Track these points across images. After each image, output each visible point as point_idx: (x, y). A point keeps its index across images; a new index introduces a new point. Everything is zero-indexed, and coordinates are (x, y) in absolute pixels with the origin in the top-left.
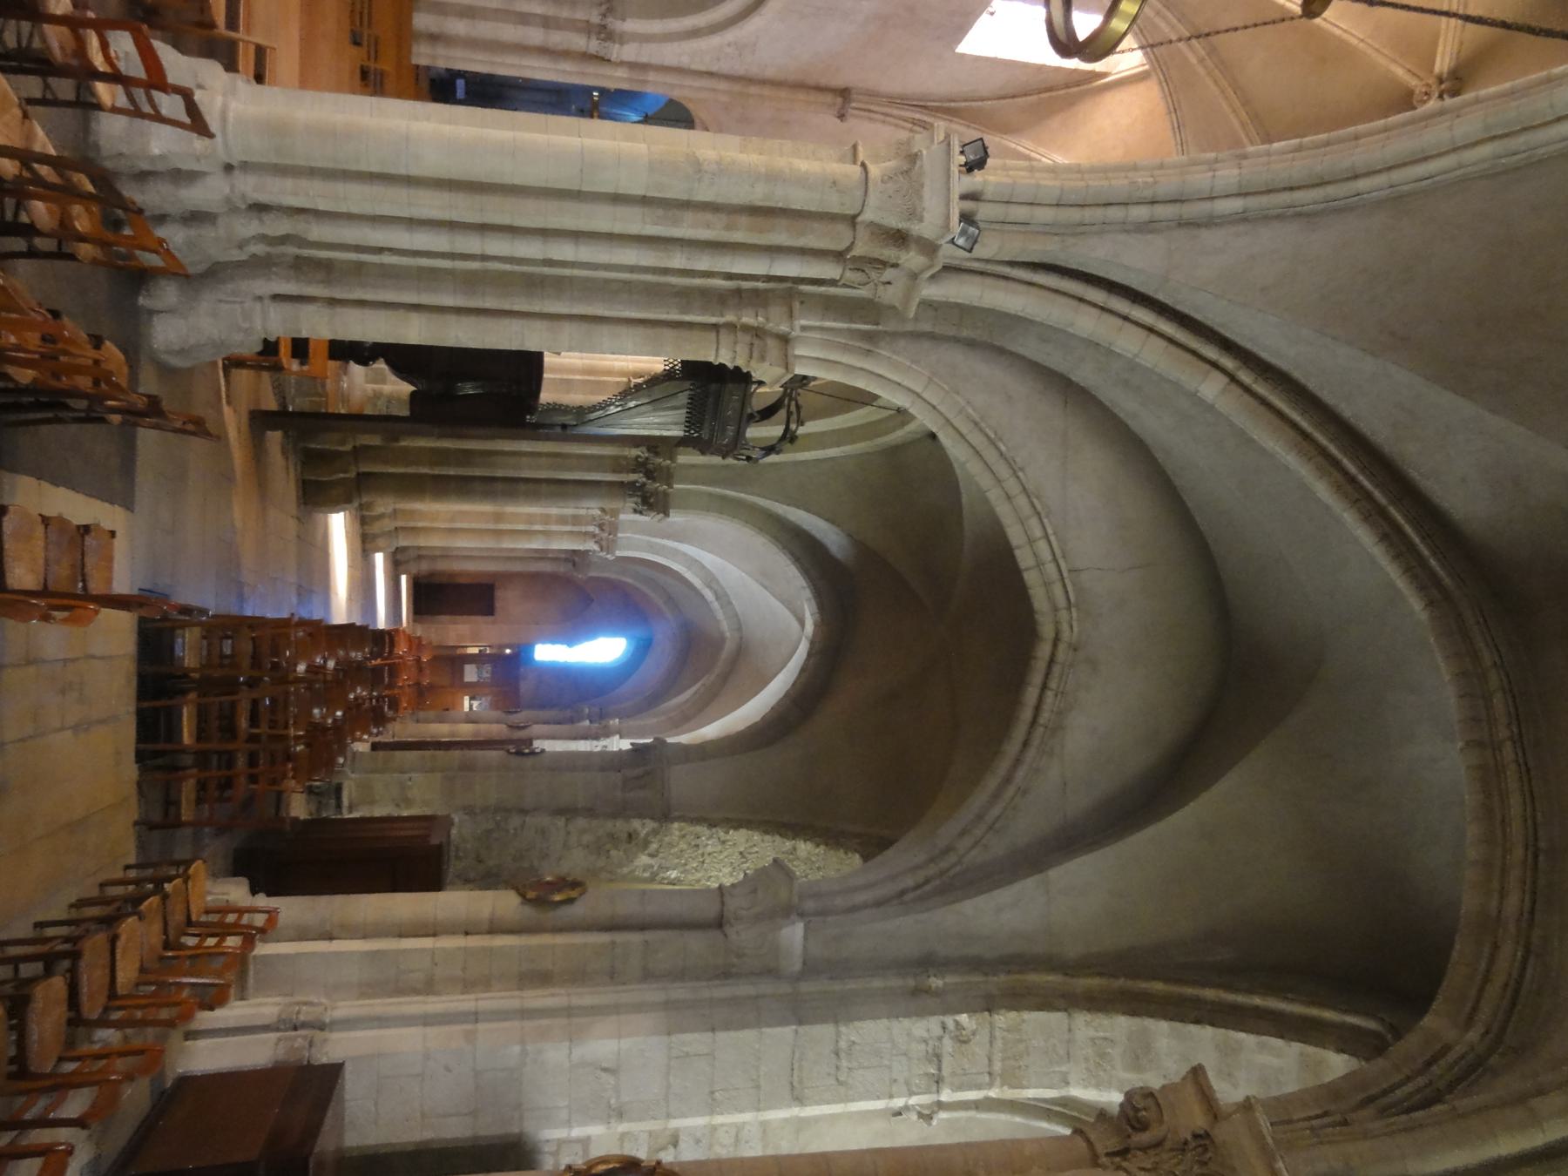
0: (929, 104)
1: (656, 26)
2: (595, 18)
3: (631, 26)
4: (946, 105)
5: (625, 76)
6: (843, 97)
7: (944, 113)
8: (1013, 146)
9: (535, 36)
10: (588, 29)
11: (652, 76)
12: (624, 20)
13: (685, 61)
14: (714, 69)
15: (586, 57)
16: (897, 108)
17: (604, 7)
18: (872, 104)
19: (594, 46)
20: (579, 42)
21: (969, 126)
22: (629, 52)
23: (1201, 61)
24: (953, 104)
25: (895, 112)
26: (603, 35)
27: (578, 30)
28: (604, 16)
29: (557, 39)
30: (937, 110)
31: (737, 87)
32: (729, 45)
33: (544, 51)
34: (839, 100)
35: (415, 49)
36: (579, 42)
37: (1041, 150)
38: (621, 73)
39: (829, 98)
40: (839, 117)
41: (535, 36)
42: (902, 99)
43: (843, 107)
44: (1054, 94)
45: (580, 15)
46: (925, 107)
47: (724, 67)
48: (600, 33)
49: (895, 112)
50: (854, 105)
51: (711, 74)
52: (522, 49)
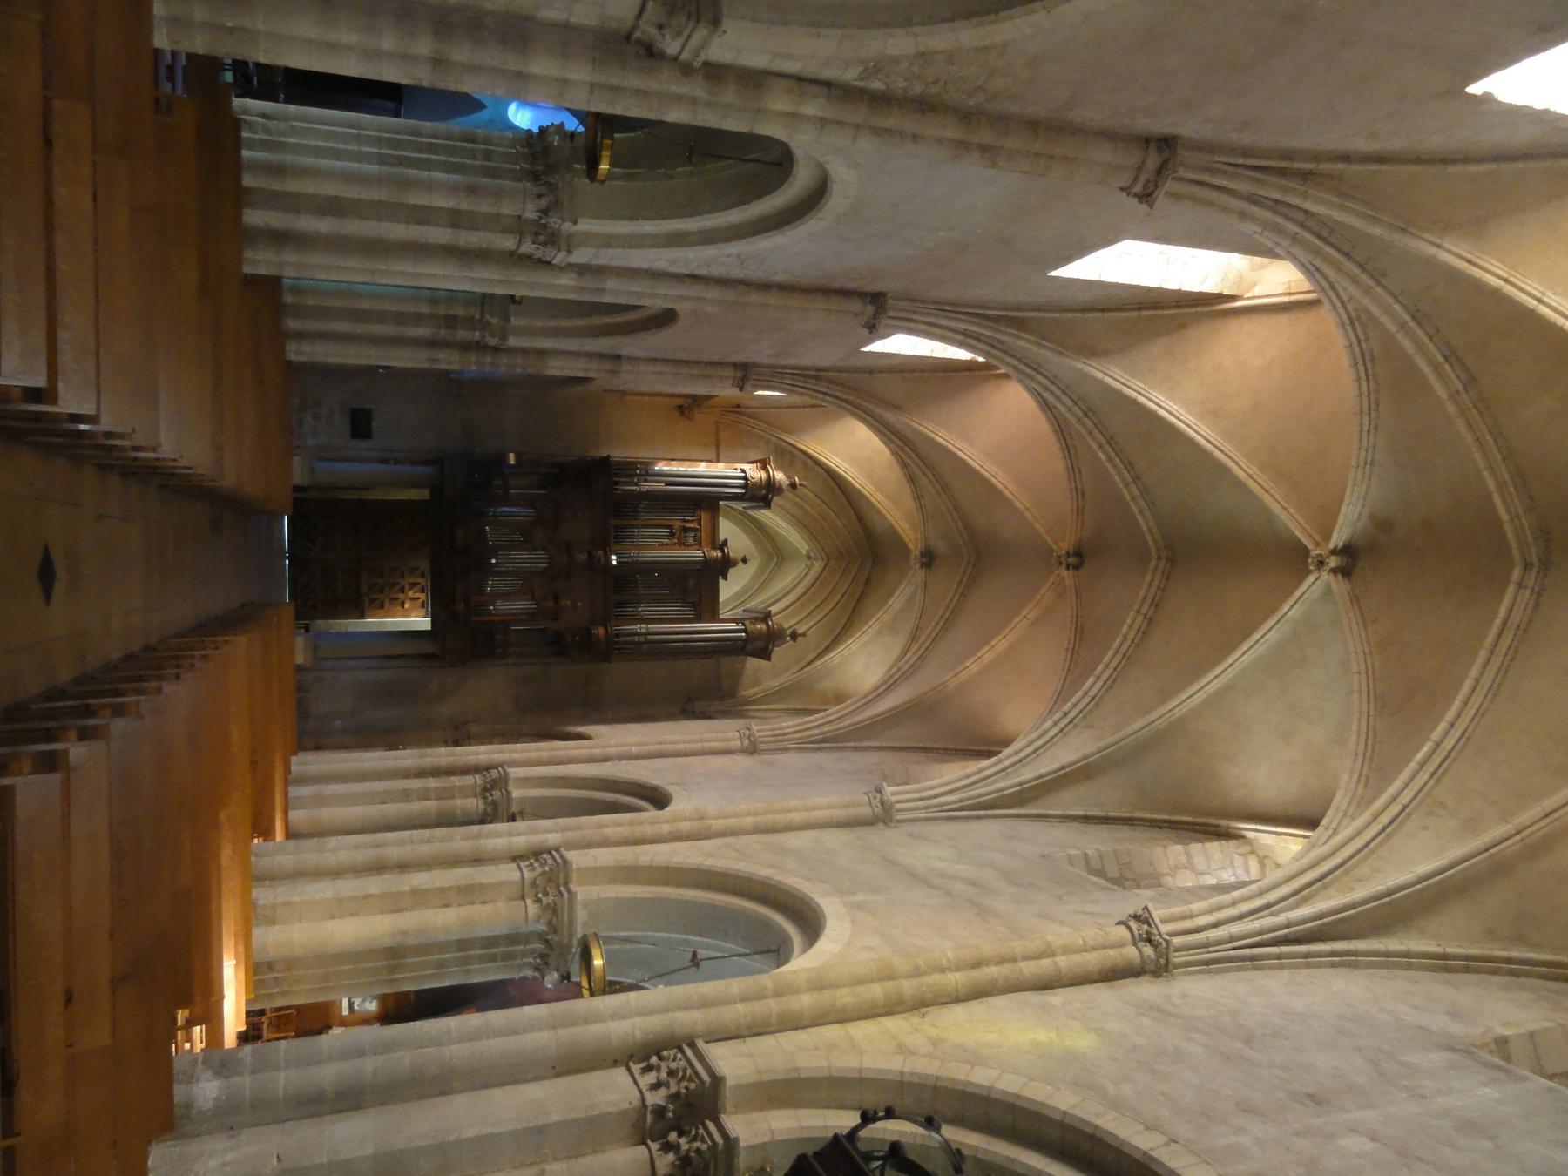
0: (988, 312)
1: (623, 227)
2: (531, 213)
3: (585, 225)
4: (1010, 314)
5: (573, 283)
6: (872, 303)
7: (1008, 326)
8: (1100, 375)
9: (439, 235)
10: (518, 227)
11: (611, 284)
12: (575, 222)
13: (661, 265)
14: (703, 272)
15: (514, 259)
16: (945, 317)
17: (544, 202)
18: (915, 312)
19: (527, 247)
20: (508, 243)
21: (1040, 345)
22: (581, 256)
23: (1455, 395)
24: (1020, 314)
25: (945, 322)
26: (541, 238)
27: (506, 230)
28: (545, 212)
29: (470, 239)
30: (997, 319)
31: (730, 295)
32: (729, 256)
33: (450, 252)
34: (870, 309)
35: (248, 254)
36: (508, 243)
37: (1139, 385)
38: (566, 280)
39: (856, 305)
40: (869, 328)
41: (439, 235)
42: (954, 304)
43: (876, 315)
44: (1159, 312)
45: (508, 209)
46: (985, 317)
47: (716, 271)
48: (537, 234)
49: (945, 322)
50: (891, 314)
51: (694, 278)
52: (420, 250)
